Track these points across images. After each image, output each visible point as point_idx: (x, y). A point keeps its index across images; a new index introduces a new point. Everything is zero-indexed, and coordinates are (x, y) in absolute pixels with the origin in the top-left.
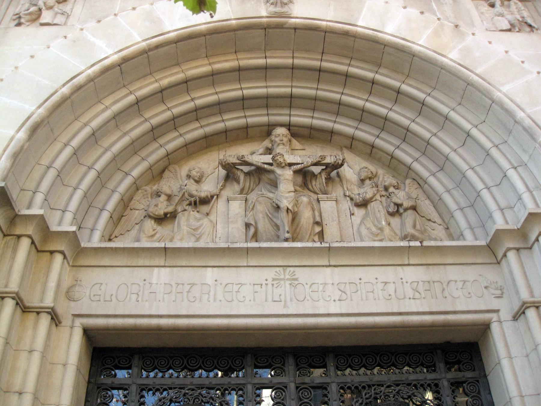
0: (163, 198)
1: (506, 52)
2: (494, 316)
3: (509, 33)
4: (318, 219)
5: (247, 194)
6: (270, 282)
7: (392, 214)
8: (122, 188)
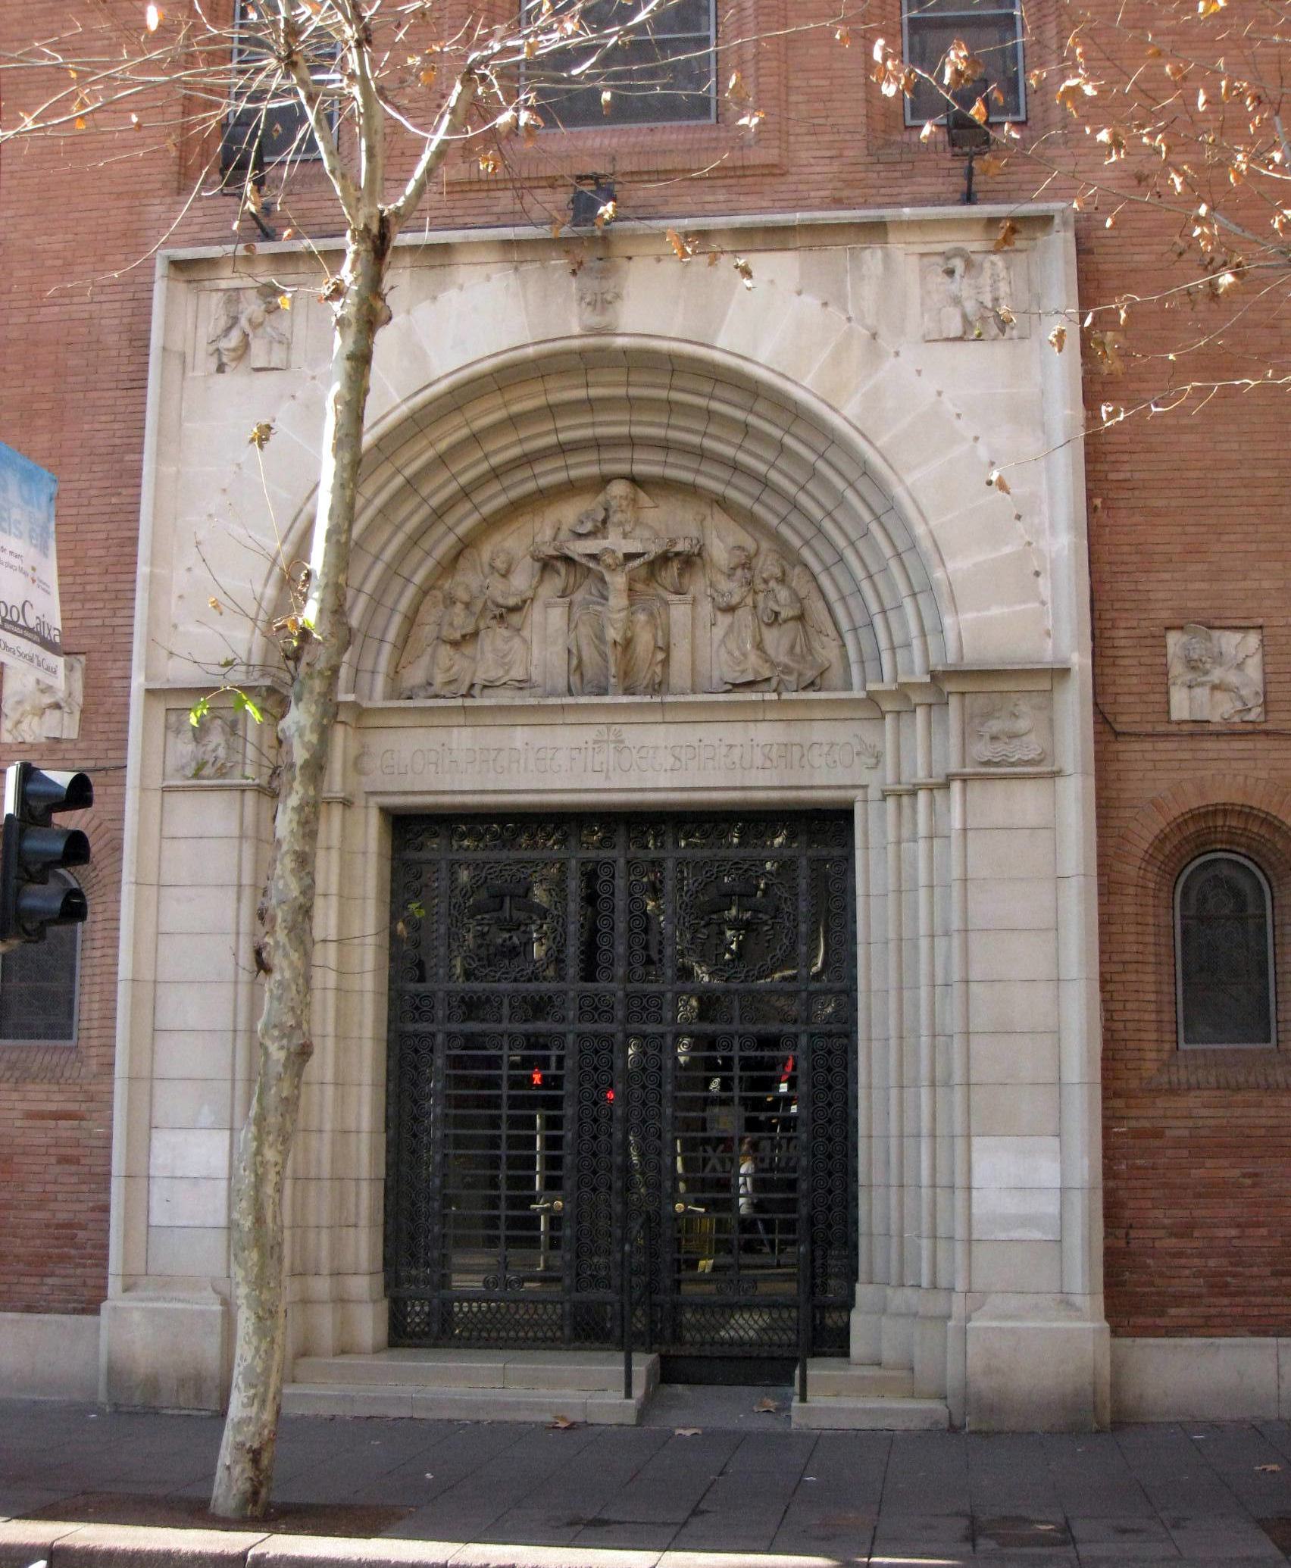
0: (459, 607)
1: (939, 393)
2: (858, 794)
3: (958, 345)
4: (660, 644)
5: (572, 592)
6: (590, 745)
7: (769, 625)
8: (404, 604)
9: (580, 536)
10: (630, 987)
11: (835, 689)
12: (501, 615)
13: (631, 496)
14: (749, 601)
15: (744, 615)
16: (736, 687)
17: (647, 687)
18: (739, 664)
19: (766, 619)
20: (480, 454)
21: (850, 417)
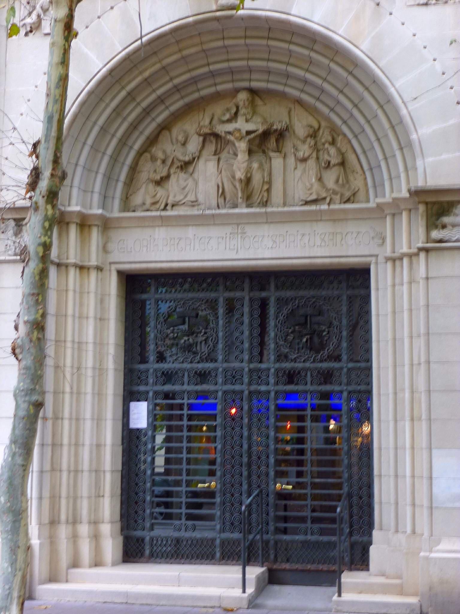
2: (373, 260)
3: (424, 8)
5: (220, 153)
6: (228, 235)
8: (129, 160)
9: (224, 122)
10: (252, 366)
11: (362, 202)
12: (181, 166)
13: (250, 99)
14: (314, 155)
15: (311, 163)
16: (307, 203)
17: (259, 203)
18: (309, 190)
19: (323, 165)
20: (168, 78)
21: (364, 50)
